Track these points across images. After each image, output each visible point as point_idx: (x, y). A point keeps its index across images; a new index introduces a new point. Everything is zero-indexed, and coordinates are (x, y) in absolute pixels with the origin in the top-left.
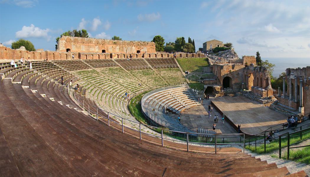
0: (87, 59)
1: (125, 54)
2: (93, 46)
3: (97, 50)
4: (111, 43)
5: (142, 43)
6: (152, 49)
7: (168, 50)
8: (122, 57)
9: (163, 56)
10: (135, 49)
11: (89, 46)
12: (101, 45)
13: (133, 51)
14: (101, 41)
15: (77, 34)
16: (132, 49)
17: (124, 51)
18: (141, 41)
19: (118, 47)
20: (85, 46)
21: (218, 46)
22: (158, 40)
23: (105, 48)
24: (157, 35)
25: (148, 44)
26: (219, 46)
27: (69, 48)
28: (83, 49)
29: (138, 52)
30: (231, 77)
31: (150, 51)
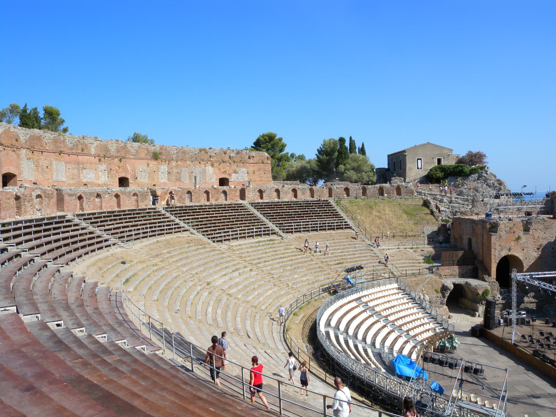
0: (82, 209)
1: (192, 188)
2: (91, 163)
3: (100, 177)
4: (143, 155)
5: (233, 155)
6: (262, 171)
7: (300, 175)
8: (184, 200)
9: (299, 193)
10: (215, 172)
11: (78, 163)
12: (116, 160)
13: (208, 179)
14: (115, 146)
15: (28, 120)
16: (204, 172)
17: (183, 179)
18: (229, 148)
19: (164, 168)
20: (66, 163)
21: (439, 161)
22: (267, 144)
23: (126, 170)
24: (266, 131)
25: (249, 158)
26: (443, 163)
27: (12, 170)
28: (61, 174)
29: (223, 182)
30: (521, 258)
31: (255, 180)
